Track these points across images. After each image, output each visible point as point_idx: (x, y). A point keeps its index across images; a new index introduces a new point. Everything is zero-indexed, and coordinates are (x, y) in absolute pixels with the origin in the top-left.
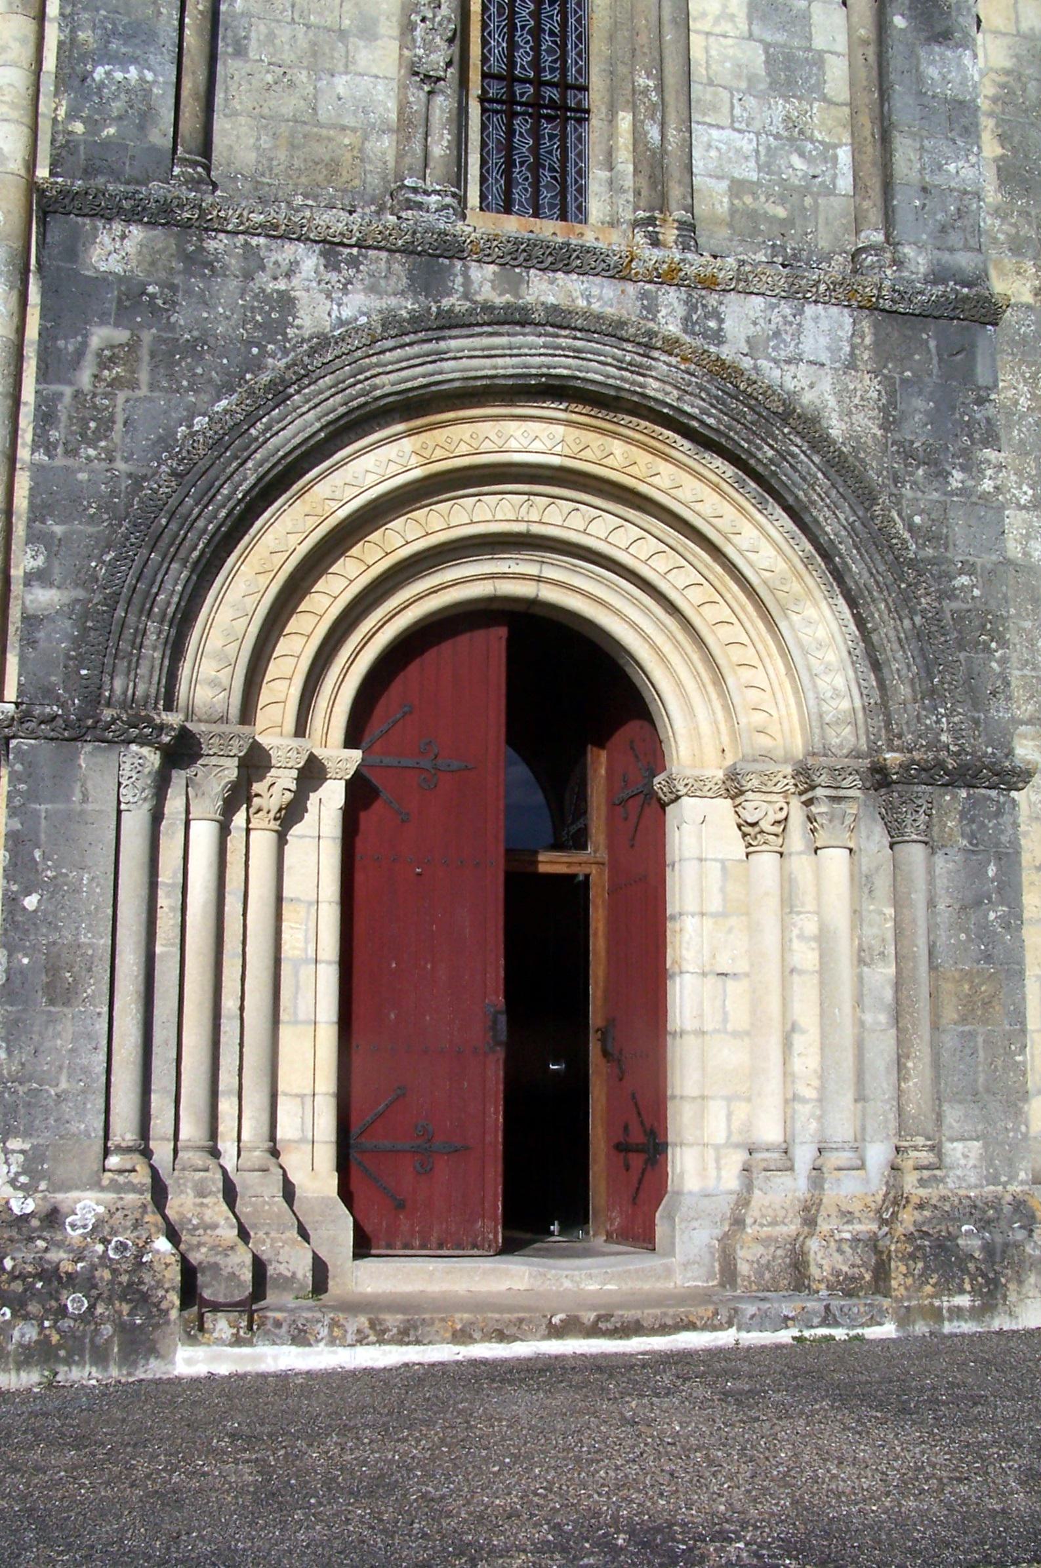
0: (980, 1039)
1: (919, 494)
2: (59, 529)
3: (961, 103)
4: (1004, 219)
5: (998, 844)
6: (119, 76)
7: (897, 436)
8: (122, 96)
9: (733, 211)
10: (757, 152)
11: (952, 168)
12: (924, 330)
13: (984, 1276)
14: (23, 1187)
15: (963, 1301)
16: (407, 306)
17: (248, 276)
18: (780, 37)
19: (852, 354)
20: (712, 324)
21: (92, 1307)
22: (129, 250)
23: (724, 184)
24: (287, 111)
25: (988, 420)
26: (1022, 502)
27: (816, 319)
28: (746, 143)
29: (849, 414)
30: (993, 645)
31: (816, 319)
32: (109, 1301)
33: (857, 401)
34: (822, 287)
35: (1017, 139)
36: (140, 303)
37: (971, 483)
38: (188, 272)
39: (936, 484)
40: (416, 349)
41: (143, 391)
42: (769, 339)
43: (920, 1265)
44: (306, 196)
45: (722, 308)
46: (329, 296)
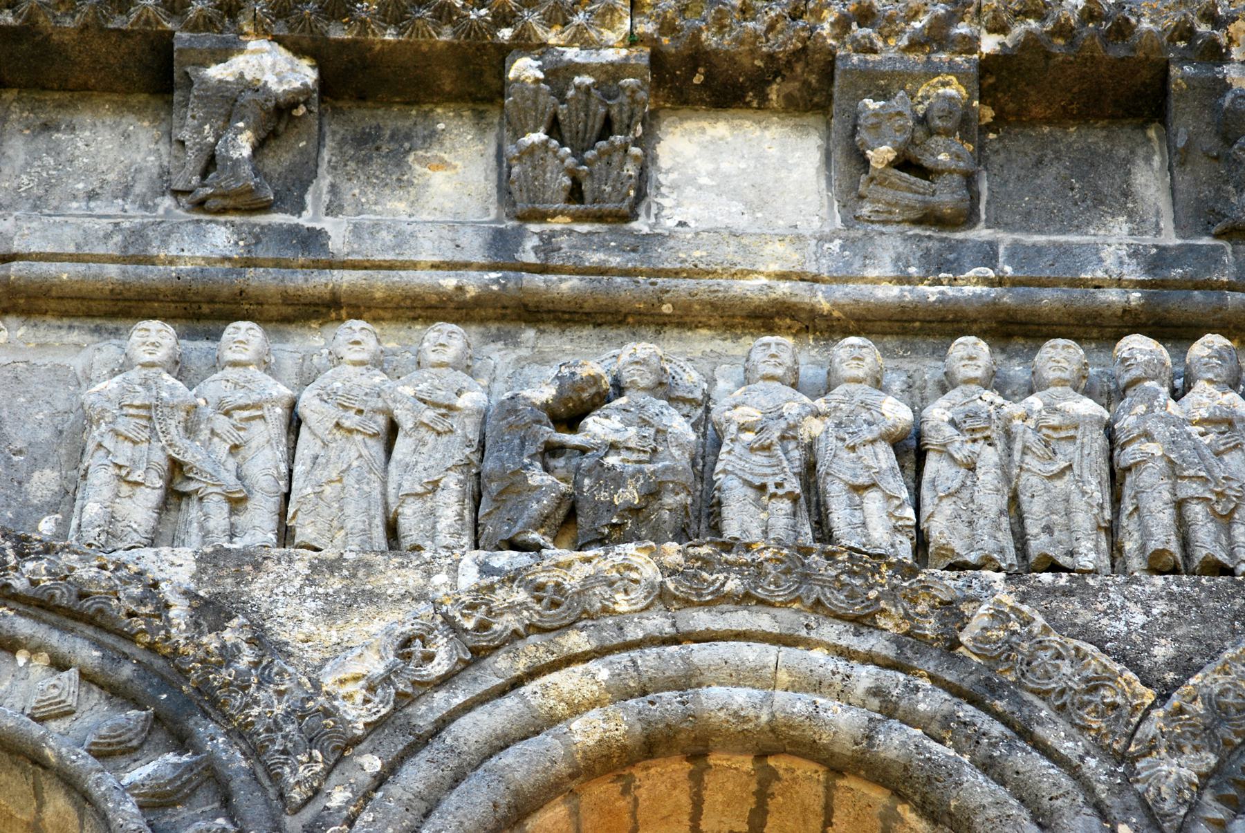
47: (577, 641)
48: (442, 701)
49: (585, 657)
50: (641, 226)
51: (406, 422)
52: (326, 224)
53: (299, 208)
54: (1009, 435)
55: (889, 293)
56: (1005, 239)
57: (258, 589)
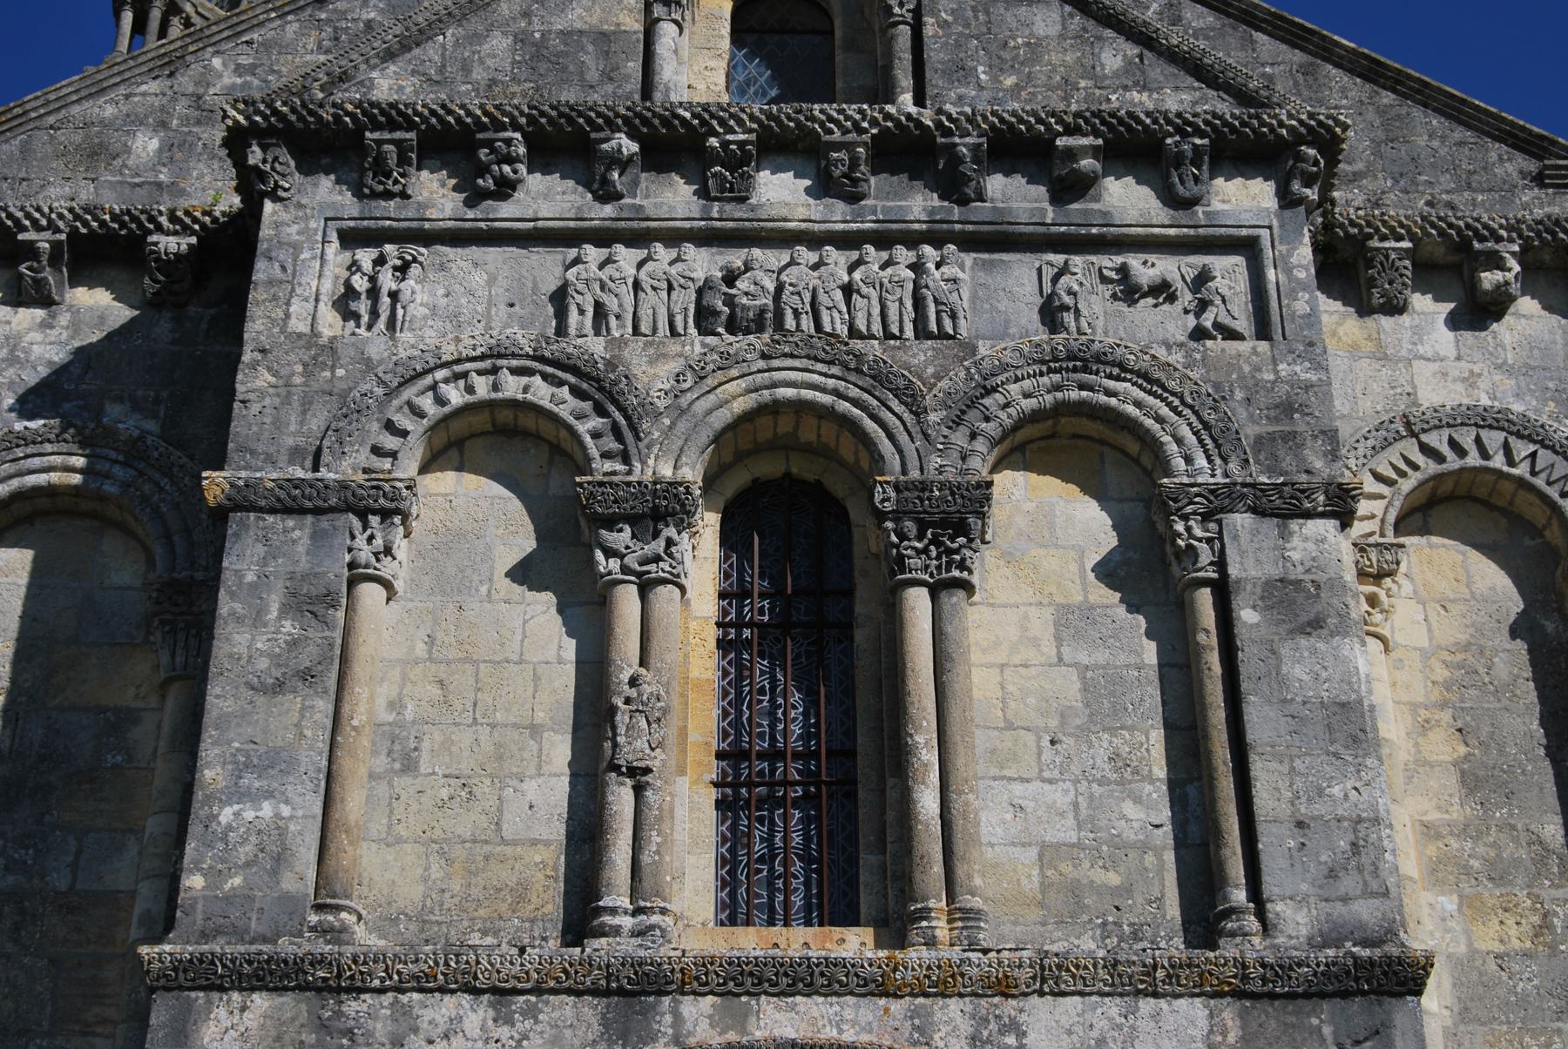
3: (1343, 705)
4: (1476, 839)
6: (249, 815)
8: (253, 839)
9: (1045, 887)
10: (1076, 805)
11: (1336, 791)
12: (1313, 1013)
18: (1101, 657)
22: (248, 1023)
23: (1033, 852)
24: (465, 830)
27: (1156, 1016)
28: (1060, 796)
31: (1156, 1016)
34: (1160, 974)
35: (1485, 730)
44: (485, 933)
45: (1023, 1018)
47: (734, 372)
48: (690, 396)
49: (737, 378)
50: (753, 201)
51: (675, 285)
52: (645, 203)
53: (635, 196)
54: (881, 285)
55: (840, 227)
56: (880, 204)
57: (626, 353)
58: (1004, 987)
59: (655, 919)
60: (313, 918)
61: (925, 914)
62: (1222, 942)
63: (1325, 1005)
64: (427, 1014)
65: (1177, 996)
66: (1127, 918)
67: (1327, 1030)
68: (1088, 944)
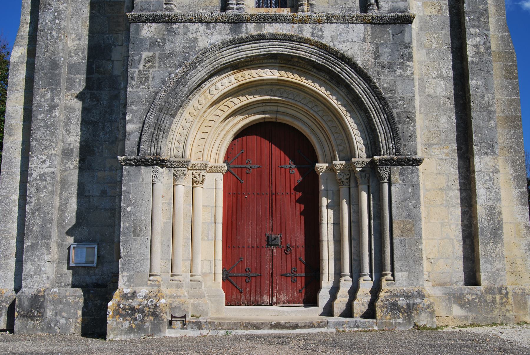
0: (407, 241)
1: (386, 78)
2: (135, 108)
5: (412, 182)
7: (379, 61)
12: (388, 27)
13: (407, 313)
14: (127, 286)
15: (400, 321)
16: (229, 37)
17: (185, 34)
19: (364, 38)
20: (320, 33)
21: (143, 318)
22: (152, 30)
25: (409, 53)
26: (434, 76)
27: (353, 28)
29: (363, 56)
30: (411, 122)
31: (353, 28)
32: (148, 316)
33: (366, 51)
34: (354, 19)
36: (155, 44)
37: (403, 73)
38: (168, 35)
39: (392, 74)
40: (232, 50)
41: (157, 69)
42: (338, 36)
43: (386, 309)
44: (203, 9)
45: (323, 28)
46: (207, 37)
58: (319, 21)
59: (241, 6)
60: (165, 6)
61: (302, 5)
62: (368, 11)
63: (390, 26)
64: (191, 28)
65: (358, 24)
66: (347, 6)
67: (390, 31)
68: (338, 12)
